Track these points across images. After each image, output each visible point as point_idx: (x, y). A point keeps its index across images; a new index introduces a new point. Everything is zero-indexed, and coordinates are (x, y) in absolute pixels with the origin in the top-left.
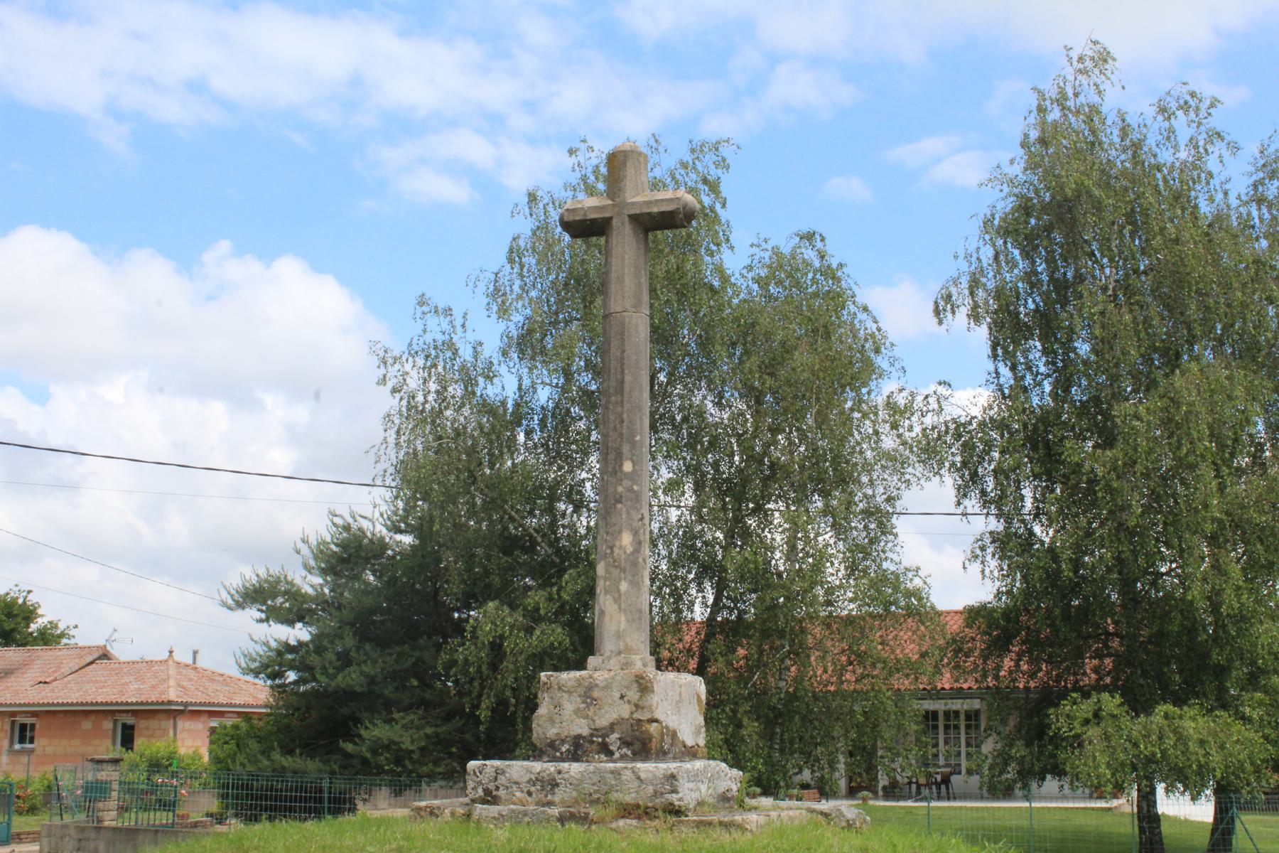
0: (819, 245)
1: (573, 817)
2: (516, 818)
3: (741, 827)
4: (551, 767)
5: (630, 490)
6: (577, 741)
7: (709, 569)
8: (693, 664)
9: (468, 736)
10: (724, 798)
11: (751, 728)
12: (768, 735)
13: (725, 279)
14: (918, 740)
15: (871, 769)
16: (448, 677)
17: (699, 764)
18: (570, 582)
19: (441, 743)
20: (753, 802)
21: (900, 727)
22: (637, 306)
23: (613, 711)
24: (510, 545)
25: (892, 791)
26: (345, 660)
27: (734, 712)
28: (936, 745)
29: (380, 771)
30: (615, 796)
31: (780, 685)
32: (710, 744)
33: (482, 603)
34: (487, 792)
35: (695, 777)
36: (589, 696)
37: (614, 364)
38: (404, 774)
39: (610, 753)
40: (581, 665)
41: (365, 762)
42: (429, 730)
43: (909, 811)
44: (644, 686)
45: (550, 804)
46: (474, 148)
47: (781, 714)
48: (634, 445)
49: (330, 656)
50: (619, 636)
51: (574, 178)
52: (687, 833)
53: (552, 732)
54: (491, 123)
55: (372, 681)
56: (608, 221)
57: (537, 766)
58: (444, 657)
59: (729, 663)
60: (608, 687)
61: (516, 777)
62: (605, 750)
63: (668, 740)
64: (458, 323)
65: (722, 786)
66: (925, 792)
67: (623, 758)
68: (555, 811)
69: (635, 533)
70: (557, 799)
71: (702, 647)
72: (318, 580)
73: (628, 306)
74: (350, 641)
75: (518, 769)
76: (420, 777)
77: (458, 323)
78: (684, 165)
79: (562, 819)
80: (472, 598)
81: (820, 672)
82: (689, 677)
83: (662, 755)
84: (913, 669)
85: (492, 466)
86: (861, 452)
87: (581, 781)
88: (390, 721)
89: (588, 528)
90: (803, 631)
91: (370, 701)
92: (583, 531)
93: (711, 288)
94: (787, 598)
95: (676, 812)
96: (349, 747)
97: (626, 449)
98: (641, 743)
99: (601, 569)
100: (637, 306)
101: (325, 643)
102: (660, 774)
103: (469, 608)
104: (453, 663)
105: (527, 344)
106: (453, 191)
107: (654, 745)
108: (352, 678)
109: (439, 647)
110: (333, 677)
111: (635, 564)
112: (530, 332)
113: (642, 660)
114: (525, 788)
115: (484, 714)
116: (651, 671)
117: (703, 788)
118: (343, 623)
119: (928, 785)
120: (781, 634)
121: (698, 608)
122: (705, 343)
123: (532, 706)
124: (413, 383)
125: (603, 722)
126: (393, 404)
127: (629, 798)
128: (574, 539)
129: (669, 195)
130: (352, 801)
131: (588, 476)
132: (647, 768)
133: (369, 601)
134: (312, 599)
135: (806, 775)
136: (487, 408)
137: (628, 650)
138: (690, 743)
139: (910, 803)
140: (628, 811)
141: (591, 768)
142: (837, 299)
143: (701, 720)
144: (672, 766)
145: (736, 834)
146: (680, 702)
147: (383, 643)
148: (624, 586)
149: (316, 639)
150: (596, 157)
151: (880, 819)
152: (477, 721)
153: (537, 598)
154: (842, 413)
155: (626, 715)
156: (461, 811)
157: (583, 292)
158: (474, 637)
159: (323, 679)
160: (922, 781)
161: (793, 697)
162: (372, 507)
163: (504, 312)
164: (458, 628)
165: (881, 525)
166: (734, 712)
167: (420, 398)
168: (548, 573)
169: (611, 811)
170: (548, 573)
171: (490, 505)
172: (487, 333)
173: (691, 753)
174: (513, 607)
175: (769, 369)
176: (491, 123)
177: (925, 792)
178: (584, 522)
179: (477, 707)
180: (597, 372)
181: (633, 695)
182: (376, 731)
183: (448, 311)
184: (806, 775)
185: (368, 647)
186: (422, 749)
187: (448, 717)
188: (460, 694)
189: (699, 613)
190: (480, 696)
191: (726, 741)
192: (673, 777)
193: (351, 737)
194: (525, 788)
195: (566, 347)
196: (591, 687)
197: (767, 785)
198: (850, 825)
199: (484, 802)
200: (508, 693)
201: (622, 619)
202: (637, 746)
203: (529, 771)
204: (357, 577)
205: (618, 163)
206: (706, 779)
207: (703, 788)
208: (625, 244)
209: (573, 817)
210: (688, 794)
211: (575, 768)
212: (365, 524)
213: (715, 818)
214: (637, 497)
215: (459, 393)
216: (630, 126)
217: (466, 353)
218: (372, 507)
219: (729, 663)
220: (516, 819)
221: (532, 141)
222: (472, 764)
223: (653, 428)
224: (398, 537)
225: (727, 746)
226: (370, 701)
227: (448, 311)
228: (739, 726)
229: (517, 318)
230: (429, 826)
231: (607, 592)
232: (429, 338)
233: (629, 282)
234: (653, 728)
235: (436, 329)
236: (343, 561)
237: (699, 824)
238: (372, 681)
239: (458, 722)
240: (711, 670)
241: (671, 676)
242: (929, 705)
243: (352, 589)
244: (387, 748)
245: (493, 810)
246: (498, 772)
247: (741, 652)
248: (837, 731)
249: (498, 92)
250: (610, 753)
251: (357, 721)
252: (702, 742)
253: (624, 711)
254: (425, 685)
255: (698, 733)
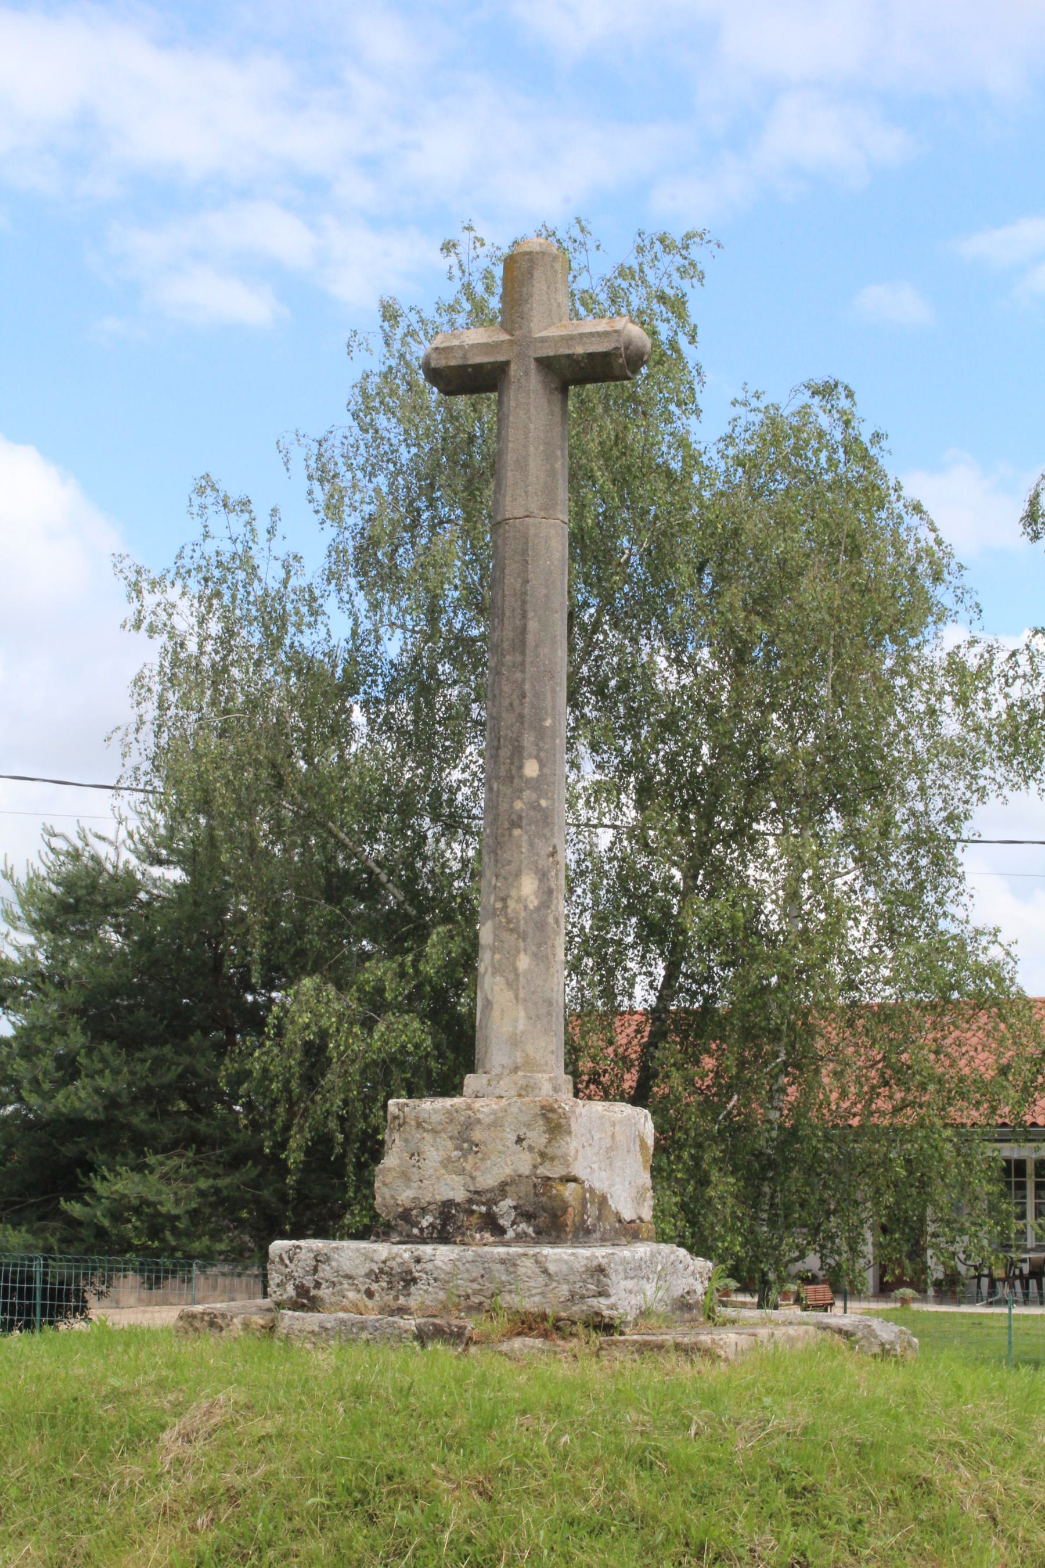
0: (844, 403)
1: (439, 1332)
2: (348, 1334)
3: (709, 1353)
4: (404, 1252)
5: (536, 807)
6: (446, 1210)
7: (659, 930)
8: (630, 1080)
9: (266, 1194)
10: (684, 1305)
11: (723, 1186)
12: (751, 1198)
13: (692, 460)
14: (993, 1208)
15: (917, 1252)
16: (235, 1098)
17: (643, 1250)
18: (437, 947)
19: (222, 1203)
20: (730, 1312)
21: (964, 1186)
22: (549, 507)
23: (505, 1163)
24: (339, 886)
25: (949, 1288)
26: (69, 1069)
27: (697, 1159)
28: (1022, 1216)
29: (127, 1246)
30: (507, 1300)
31: (768, 1118)
32: (660, 1212)
33: (292, 981)
34: (302, 1290)
35: (636, 1270)
36: (466, 1139)
37: (510, 602)
38: (160, 1254)
39: (499, 1231)
40: (449, 1086)
41: (101, 1233)
42: (203, 1184)
43: (977, 1322)
44: (554, 1123)
45: (402, 1311)
46: (282, 235)
47: (771, 1164)
48: (541, 733)
49: (46, 1062)
50: (515, 1041)
51: (450, 292)
52: (622, 1360)
53: (405, 1196)
54: (308, 193)
55: (112, 1102)
56: (502, 368)
57: (381, 1250)
58: (229, 1066)
59: (689, 1081)
60: (496, 1124)
61: (347, 1267)
62: (492, 1225)
63: (592, 1210)
64: (262, 524)
65: (680, 1285)
66: (1003, 1290)
67: (520, 1238)
68: (410, 1323)
69: (543, 876)
70: (413, 1303)
71: (647, 1050)
72: (27, 939)
73: (533, 505)
74: (77, 1039)
75: (350, 1254)
76: (189, 1257)
77: (262, 524)
78: (624, 272)
79: (421, 1337)
80: (284, 965)
81: (838, 1094)
82: (624, 1110)
83: (583, 1234)
84: (988, 1093)
85: (308, 757)
86: (908, 742)
87: (452, 1275)
88: (140, 1168)
89: (465, 862)
90: (811, 1031)
91: (109, 1135)
92: (456, 866)
93: (669, 473)
94: (784, 977)
95: (607, 1327)
96: (75, 1209)
97: (528, 740)
98: (549, 1215)
99: (486, 932)
100: (549, 507)
101: (38, 1042)
102: (579, 1266)
103: (270, 985)
104: (245, 1075)
105: (371, 562)
106: (251, 307)
107: (570, 1218)
108: (79, 1098)
109: (221, 1049)
110: (49, 1096)
111: (541, 926)
112: (374, 542)
113: (552, 1081)
114: (363, 1284)
115: (294, 1157)
116: (566, 1099)
117: (650, 1288)
118: (66, 1011)
119: (1009, 1279)
120: (775, 1035)
121: (639, 992)
122: (658, 560)
123: (376, 1151)
124: (184, 622)
125: (488, 1180)
126: (148, 653)
127: (530, 1304)
128: (442, 878)
129: (602, 326)
130: (80, 1296)
131: (463, 775)
132: (558, 1255)
133: (109, 972)
134: (17, 970)
135: (812, 1262)
136: (302, 666)
137: (530, 1065)
138: (628, 1215)
139: (979, 1309)
140: (527, 1324)
141: (470, 1253)
142: (872, 493)
143: (646, 1179)
144: (599, 1253)
145: (703, 1365)
146: (612, 1149)
147: (131, 1042)
148: (524, 962)
149: (24, 1034)
150: (485, 261)
151: (934, 1338)
152: (283, 1169)
153: (379, 971)
154: (876, 678)
155: (525, 1170)
156: (259, 1320)
157: (464, 475)
158: (280, 1032)
159: (34, 1100)
160: (999, 1273)
161: (792, 1135)
162: (114, 824)
163: (333, 510)
164: (254, 1020)
165: (937, 861)
166: (697, 1159)
167: (192, 647)
168: (401, 932)
169: (501, 1323)
170: (401, 932)
171: (307, 821)
172: (305, 542)
173: (631, 1232)
174: (341, 986)
175: (761, 604)
176: (308, 193)
177: (1003, 1290)
178: (457, 852)
179: (283, 1146)
180: (478, 604)
181: (537, 1137)
182: (121, 1184)
183: (245, 504)
184: (812, 1262)
185: (106, 1048)
186: (194, 1215)
187: (235, 1163)
188: (256, 1126)
189: (643, 997)
190: (287, 1128)
191: (683, 1206)
192: (601, 1270)
193: (77, 1191)
194: (363, 1284)
195: (431, 564)
196: (469, 1125)
197: (752, 1277)
198: (885, 1352)
199: (296, 1306)
200: (333, 1124)
201: (522, 1008)
202: (543, 1219)
203: (368, 1258)
204: (88, 936)
205: (520, 270)
206: (654, 1275)
207: (650, 1288)
208: (529, 403)
209: (439, 1332)
210: (624, 1299)
211: (442, 1255)
212: (103, 850)
213: (669, 1338)
214: (546, 818)
215: (257, 638)
216: (532, 202)
217: (271, 575)
218: (114, 824)
219: (689, 1081)
220: (348, 1334)
221: (376, 223)
222: (278, 1246)
223: (573, 701)
224: (156, 871)
225: (687, 1223)
226: (109, 1135)
227: (245, 504)
228: (704, 1182)
229: (353, 519)
230: (208, 1344)
231: (496, 970)
232: (209, 548)
233: (535, 468)
234: (569, 1191)
235: (224, 533)
236: (66, 908)
237: (643, 1348)
238: (112, 1102)
239: (251, 1170)
240: (659, 1090)
241: (599, 1107)
242: (1011, 1151)
243: (81, 956)
244: (137, 1211)
245: (311, 1320)
246: (319, 1259)
247: (708, 1062)
248: (863, 1190)
249: (315, 141)
250: (499, 1231)
251: (90, 1168)
252: (647, 1214)
253: (523, 1163)
254: (198, 1110)
255: (640, 1199)
